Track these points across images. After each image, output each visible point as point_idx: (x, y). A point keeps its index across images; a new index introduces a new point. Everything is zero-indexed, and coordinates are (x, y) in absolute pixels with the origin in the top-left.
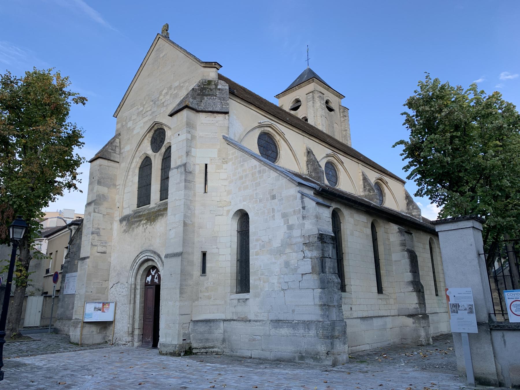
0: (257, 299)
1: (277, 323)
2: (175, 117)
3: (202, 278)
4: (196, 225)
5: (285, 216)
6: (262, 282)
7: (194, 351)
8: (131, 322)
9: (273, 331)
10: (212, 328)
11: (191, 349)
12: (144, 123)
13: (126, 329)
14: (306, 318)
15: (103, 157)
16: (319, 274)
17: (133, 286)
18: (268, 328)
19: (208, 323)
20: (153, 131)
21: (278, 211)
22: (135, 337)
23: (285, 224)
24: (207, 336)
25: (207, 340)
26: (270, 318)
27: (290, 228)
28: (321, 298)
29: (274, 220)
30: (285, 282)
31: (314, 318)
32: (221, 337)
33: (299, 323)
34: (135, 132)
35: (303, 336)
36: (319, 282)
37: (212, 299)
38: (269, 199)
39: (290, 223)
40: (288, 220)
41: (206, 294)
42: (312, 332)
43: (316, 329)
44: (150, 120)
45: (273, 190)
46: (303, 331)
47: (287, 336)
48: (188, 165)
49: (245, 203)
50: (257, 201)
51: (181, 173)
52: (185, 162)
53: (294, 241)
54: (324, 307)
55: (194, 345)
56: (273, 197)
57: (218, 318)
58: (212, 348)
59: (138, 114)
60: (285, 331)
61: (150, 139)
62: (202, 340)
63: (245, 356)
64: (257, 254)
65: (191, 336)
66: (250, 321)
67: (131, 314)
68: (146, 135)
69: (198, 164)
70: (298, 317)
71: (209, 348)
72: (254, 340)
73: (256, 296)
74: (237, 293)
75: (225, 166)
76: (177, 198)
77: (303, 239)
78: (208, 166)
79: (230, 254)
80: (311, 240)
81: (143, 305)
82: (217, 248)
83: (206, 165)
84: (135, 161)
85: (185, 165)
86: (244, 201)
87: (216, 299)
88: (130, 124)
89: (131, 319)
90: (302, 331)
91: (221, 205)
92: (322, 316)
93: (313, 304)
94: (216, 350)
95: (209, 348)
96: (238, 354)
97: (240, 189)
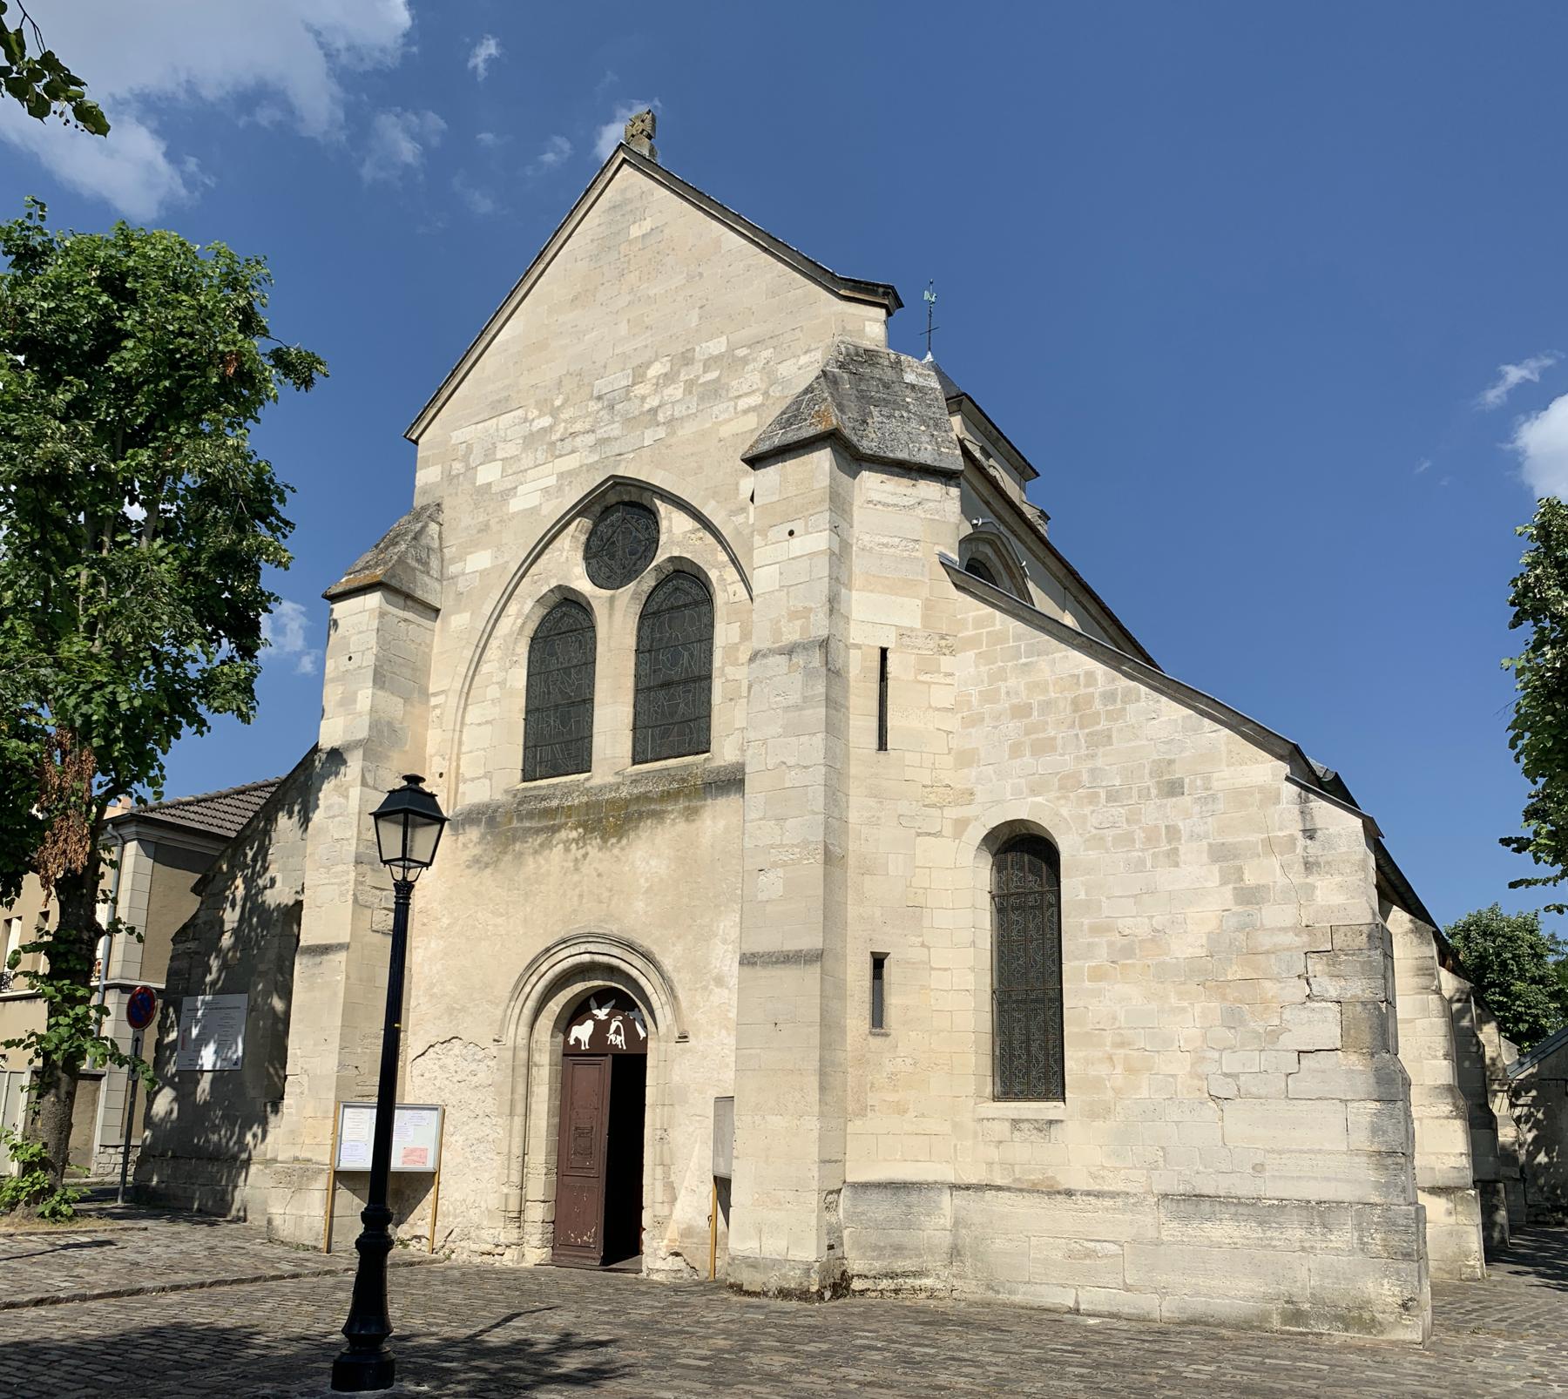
0: (1099, 1124)
1: (1192, 1203)
2: (771, 474)
3: (875, 1042)
4: (852, 861)
5: (1221, 854)
6: (1119, 1070)
7: (857, 1285)
8: (515, 1178)
9: (1172, 1230)
10: (915, 1210)
11: (845, 1278)
12: (561, 476)
13: (494, 1201)
14: (1313, 1191)
15: (393, 582)
16: (1372, 1055)
17: (523, 1055)
18: (1149, 1220)
19: (902, 1194)
20: (597, 509)
21: (1193, 837)
22: (528, 1228)
23: (1224, 883)
24: (897, 1236)
25: (899, 1249)
26: (1159, 1188)
27: (1250, 896)
28: (1375, 1130)
29: (1177, 865)
30: (1226, 1075)
31: (1345, 1193)
32: (945, 1240)
33: (1282, 1206)
34: (515, 505)
35: (1303, 1249)
36: (1372, 1080)
37: (911, 1114)
38: (1154, 792)
39: (1250, 879)
40: (1240, 870)
41: (892, 1097)
42: (1344, 1236)
43: (1359, 1227)
44: (590, 467)
45: (1170, 762)
46: (1300, 1233)
47: (1234, 1246)
48: (832, 644)
49: (1039, 799)
50: (1097, 795)
51: (809, 673)
52: (824, 633)
53: (1266, 942)
54: (1389, 1161)
55: (855, 1265)
56: (1174, 788)
57: (931, 1179)
58: (915, 1274)
59: (530, 440)
60: (1223, 1230)
61: (583, 538)
62: (882, 1249)
63: (1048, 1305)
64: (1097, 975)
65: (846, 1233)
66: (1069, 1193)
67: (517, 1151)
68: (568, 524)
69: (858, 647)
70: (1272, 1189)
71: (905, 1275)
72: (1087, 1256)
73: (1096, 1112)
74: (996, 1098)
75: (946, 662)
76: (791, 761)
77: (1305, 938)
78: (889, 655)
79: (972, 969)
80: (1339, 941)
81: (557, 1120)
82: (923, 945)
83: (884, 651)
84: (512, 608)
85: (824, 644)
86: (1034, 792)
87: (923, 1115)
88: (488, 474)
89: (516, 1166)
90: (1297, 1233)
91: (933, 799)
92: (1378, 1186)
93: (1345, 1149)
94: (928, 1282)
95: (905, 1275)
96: (1017, 1299)
97: (1016, 751)
